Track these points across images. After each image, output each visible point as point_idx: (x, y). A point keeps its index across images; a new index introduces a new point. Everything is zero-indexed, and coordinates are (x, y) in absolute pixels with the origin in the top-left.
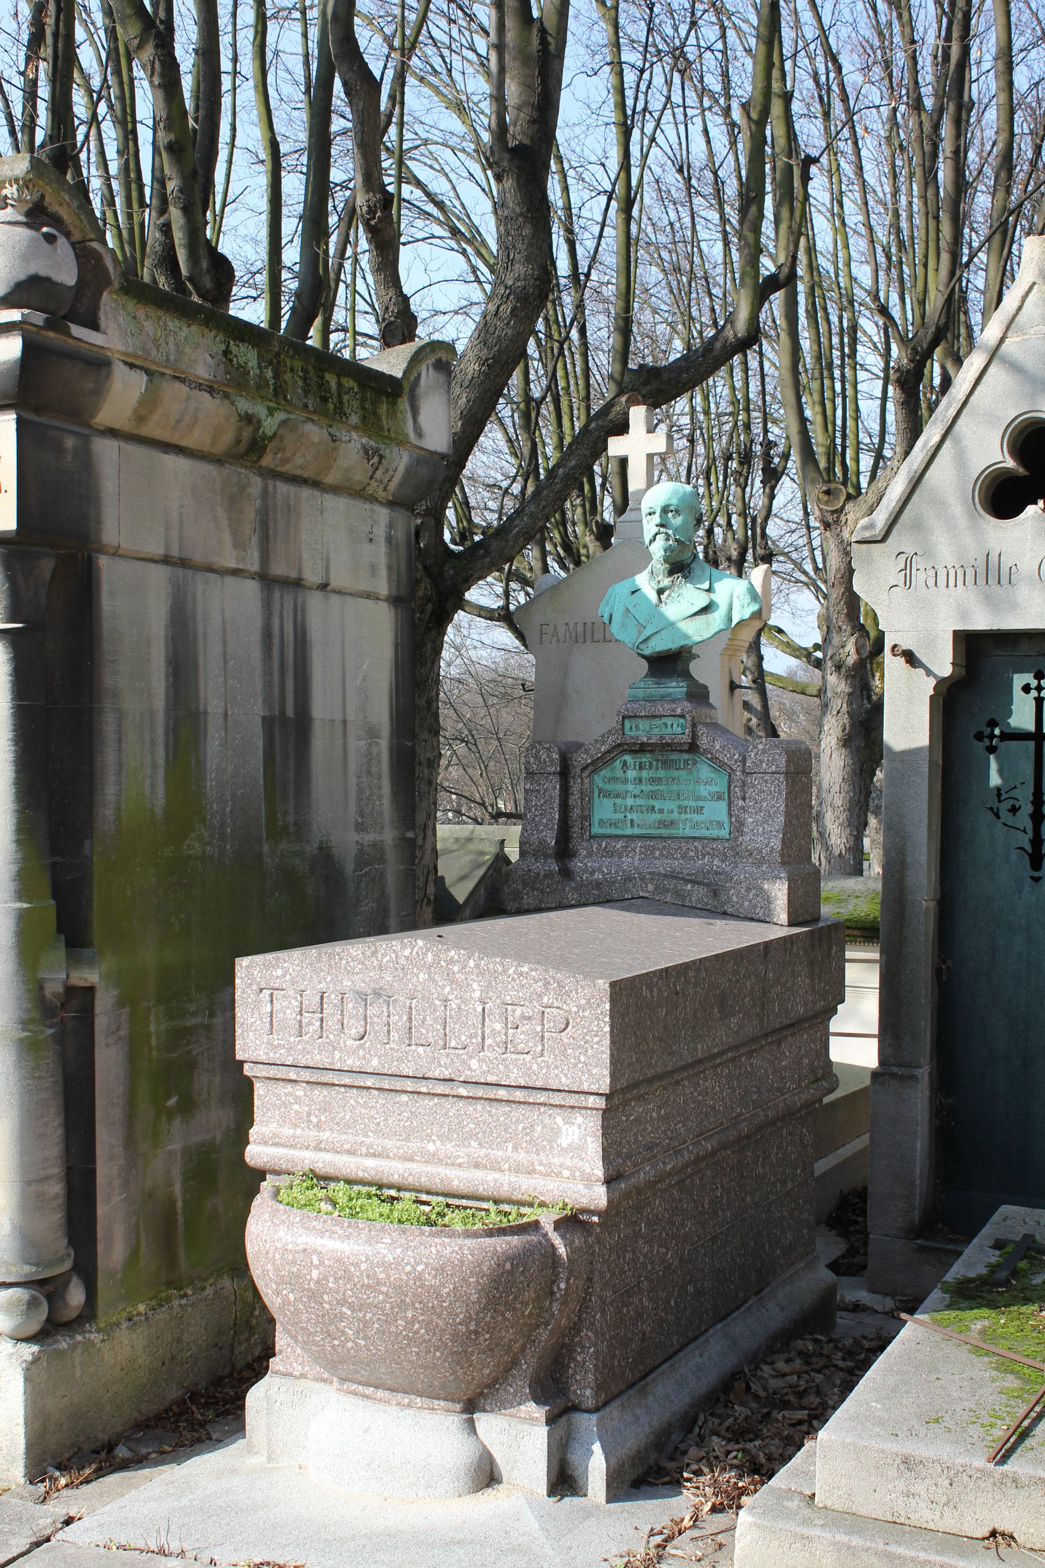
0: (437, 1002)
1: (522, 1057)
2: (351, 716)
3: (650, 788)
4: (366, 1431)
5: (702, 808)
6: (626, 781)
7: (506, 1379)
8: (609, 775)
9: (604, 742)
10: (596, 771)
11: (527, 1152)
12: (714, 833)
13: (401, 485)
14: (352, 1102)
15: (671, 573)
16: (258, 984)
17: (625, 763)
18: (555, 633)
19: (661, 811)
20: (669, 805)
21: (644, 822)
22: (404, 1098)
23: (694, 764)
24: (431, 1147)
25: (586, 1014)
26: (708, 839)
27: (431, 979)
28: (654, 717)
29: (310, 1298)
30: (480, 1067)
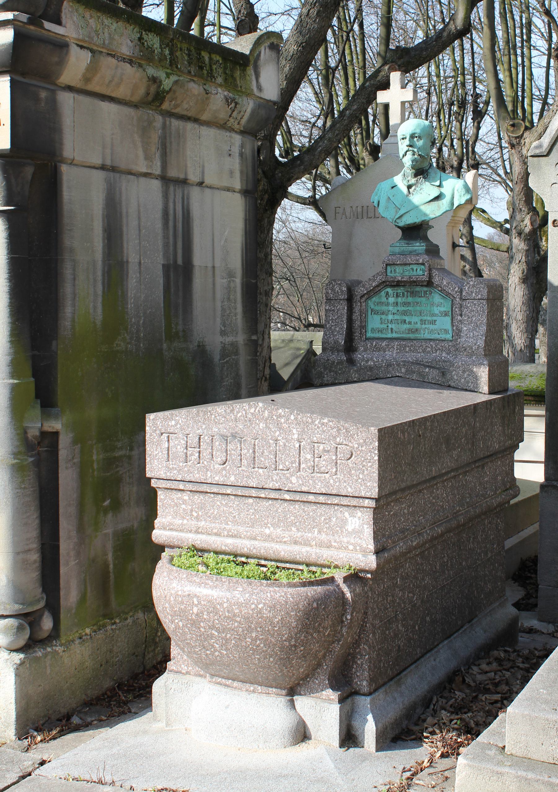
0: (271, 441)
1: (323, 475)
2: (217, 265)
3: (403, 308)
4: (227, 707)
5: (435, 321)
6: (388, 304)
7: (314, 675)
8: (377, 300)
9: (374, 280)
10: (369, 298)
11: (327, 534)
12: (443, 336)
13: (249, 121)
14: (218, 503)
15: (416, 175)
16: (160, 430)
17: (387, 293)
18: (344, 213)
19: (410, 323)
20: (414, 319)
21: (399, 330)
22: (251, 501)
23: (430, 294)
24: (267, 531)
25: (363, 449)
26: (439, 340)
27: (267, 427)
28: (406, 264)
29: (192, 624)
30: (298, 481)
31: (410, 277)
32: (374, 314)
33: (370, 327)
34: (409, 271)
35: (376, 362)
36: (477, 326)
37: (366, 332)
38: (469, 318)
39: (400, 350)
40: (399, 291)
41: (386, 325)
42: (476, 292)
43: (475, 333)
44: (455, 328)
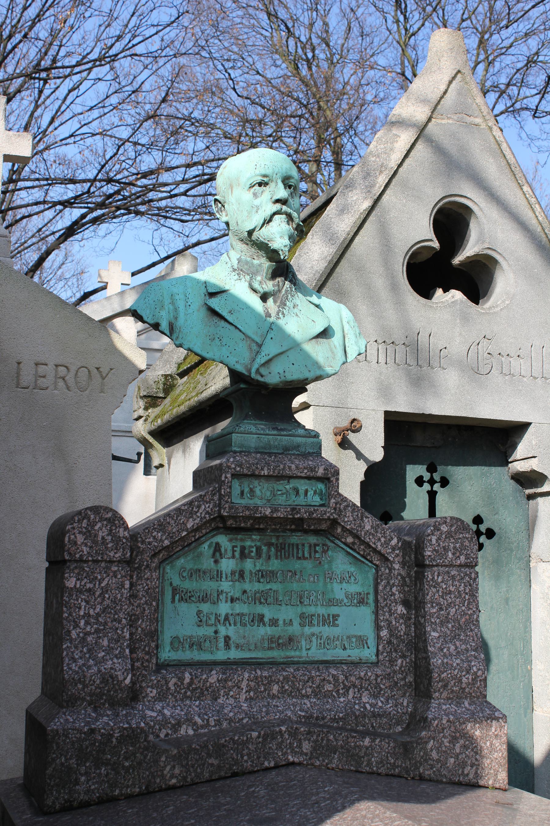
3: (257, 586)
5: (335, 617)
6: (219, 576)
8: (190, 566)
9: (192, 514)
12: (354, 654)
17: (217, 547)
19: (274, 622)
20: (286, 613)
21: (244, 640)
23: (325, 552)
31: (293, 509)
32: (181, 599)
33: (167, 637)
35: (202, 727)
36: (460, 628)
37: (157, 647)
38: (441, 609)
39: (256, 691)
40: (248, 543)
41: (213, 629)
42: (455, 548)
43: (458, 643)
44: (384, 633)
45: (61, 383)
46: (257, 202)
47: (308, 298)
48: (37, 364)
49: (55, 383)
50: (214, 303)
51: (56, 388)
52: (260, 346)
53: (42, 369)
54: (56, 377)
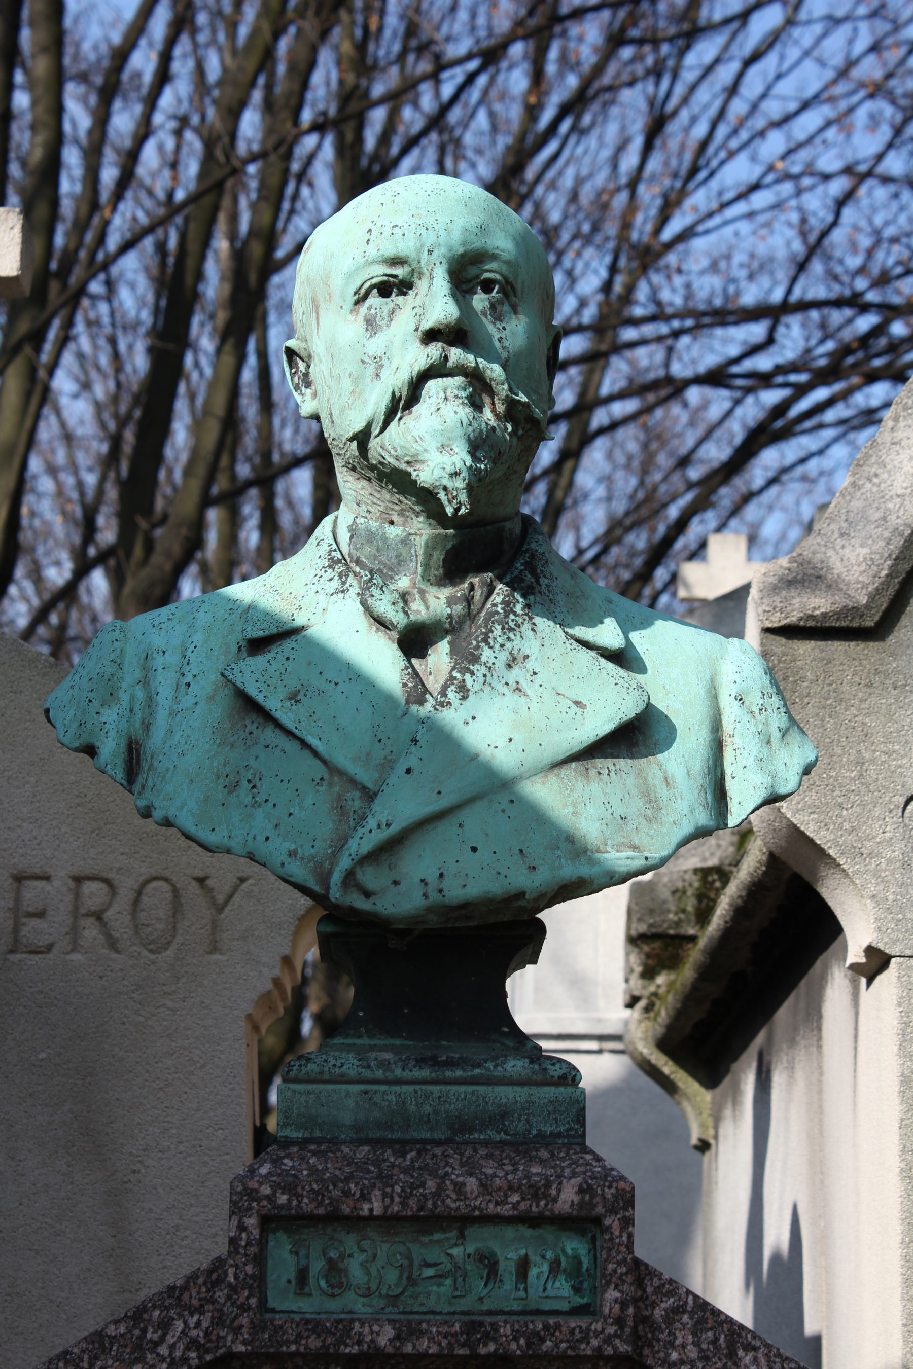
15: (453, 566)
28: (428, 1222)
31: (472, 1327)
34: (457, 1272)
45: (91, 932)
46: (375, 345)
47: (580, 631)
48: (19, 879)
49: (75, 932)
50: (253, 675)
51: (75, 947)
52: (370, 796)
53: (33, 892)
54: (76, 912)
